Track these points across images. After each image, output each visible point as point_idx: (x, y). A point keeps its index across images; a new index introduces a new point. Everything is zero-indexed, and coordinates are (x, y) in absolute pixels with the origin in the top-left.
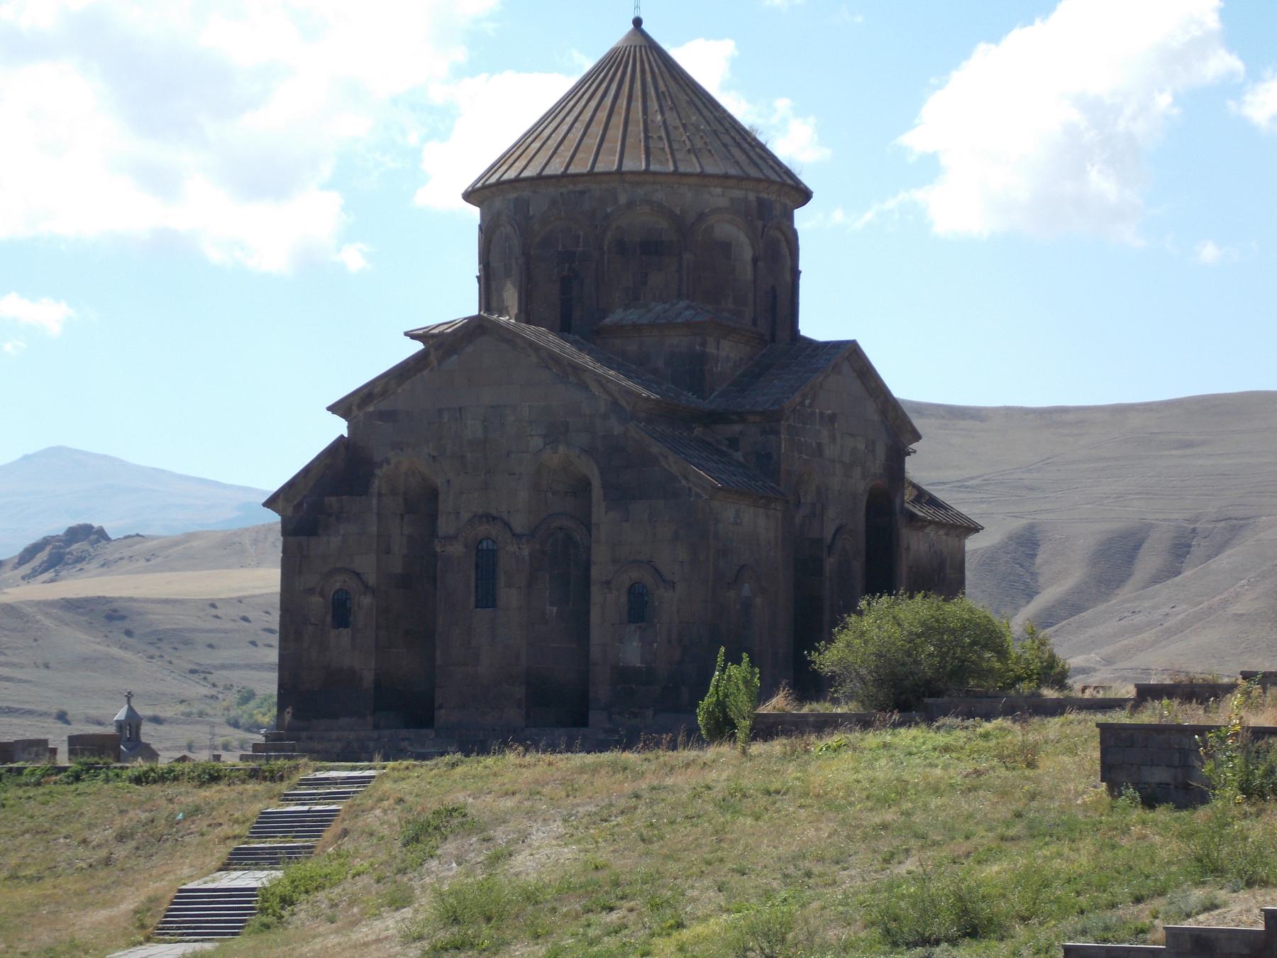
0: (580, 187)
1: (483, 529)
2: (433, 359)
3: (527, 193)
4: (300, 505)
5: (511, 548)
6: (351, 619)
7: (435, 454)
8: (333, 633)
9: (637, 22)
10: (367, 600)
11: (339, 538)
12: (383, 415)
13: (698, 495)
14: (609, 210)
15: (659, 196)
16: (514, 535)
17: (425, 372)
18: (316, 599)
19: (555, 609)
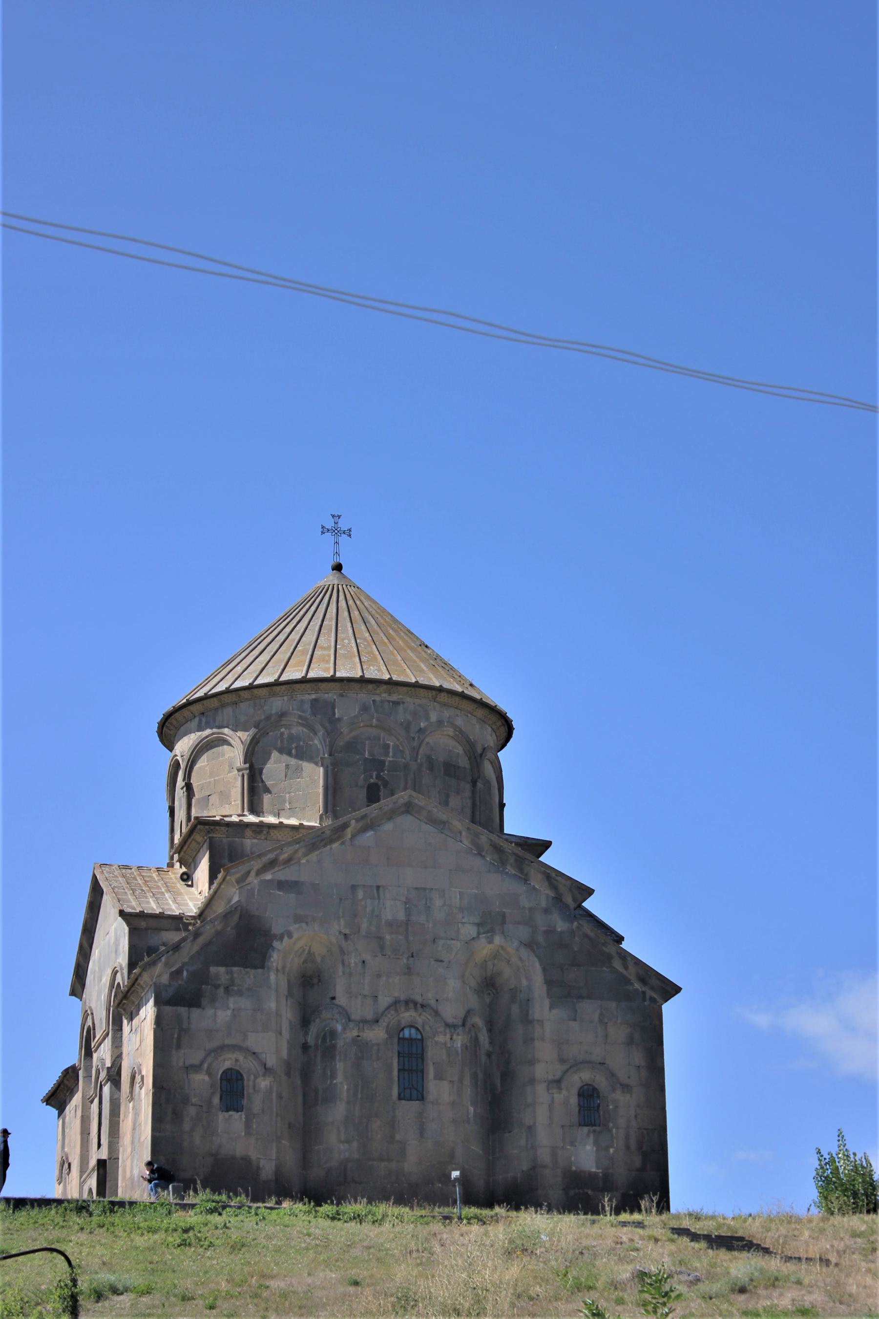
0: (394, 697)
1: (407, 1016)
2: (349, 832)
3: (330, 696)
4: (179, 972)
5: (441, 1039)
6: (245, 1102)
7: (347, 931)
8: (222, 1116)
9: (338, 568)
10: (264, 1083)
11: (229, 1012)
12: (282, 885)
14: (422, 725)
15: (459, 722)
16: (447, 1025)
17: (335, 845)
18: (201, 1078)
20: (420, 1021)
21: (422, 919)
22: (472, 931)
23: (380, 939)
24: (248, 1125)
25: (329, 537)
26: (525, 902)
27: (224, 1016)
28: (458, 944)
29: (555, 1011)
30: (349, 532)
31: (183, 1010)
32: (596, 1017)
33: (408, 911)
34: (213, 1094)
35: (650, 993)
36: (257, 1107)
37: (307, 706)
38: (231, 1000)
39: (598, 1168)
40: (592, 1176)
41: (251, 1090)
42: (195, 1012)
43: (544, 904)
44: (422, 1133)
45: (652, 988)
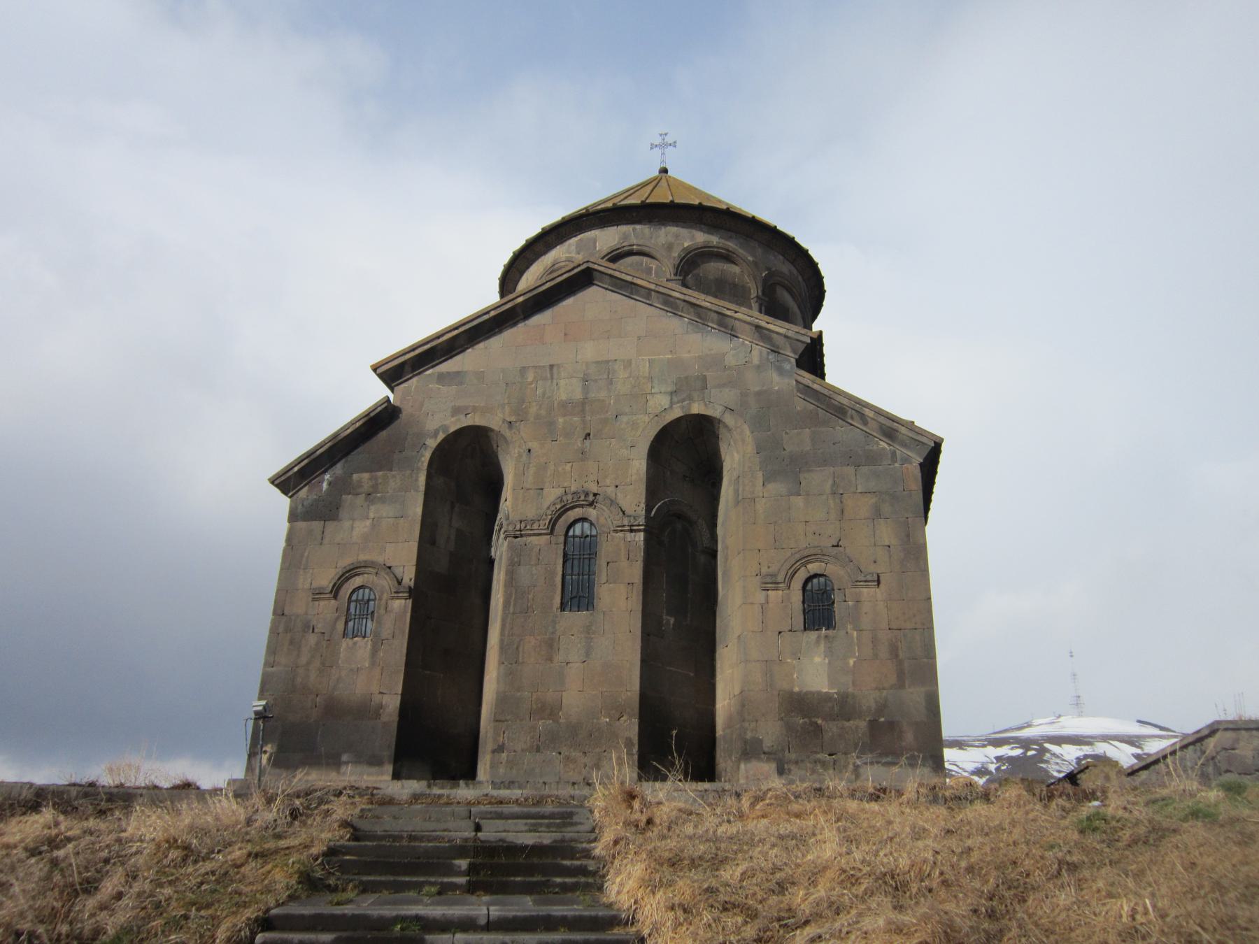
7: (513, 419)
8: (345, 643)
9: (664, 171)
10: (398, 602)
11: (368, 523)
12: (441, 378)
13: (906, 460)
14: (686, 245)
19: (672, 620)
20: (592, 513)
21: (603, 394)
22: (664, 401)
23: (551, 424)
24: (374, 652)
25: (657, 151)
26: (730, 360)
27: (362, 527)
28: (647, 419)
29: (770, 486)
30: (674, 144)
31: (317, 525)
32: (828, 487)
33: (586, 388)
34: (337, 619)
35: (901, 451)
36: (385, 633)
37: (573, 248)
38: (373, 508)
39: (831, 685)
40: (827, 698)
41: (382, 611)
42: (331, 525)
43: (756, 361)
44: (588, 654)
45: (904, 445)
